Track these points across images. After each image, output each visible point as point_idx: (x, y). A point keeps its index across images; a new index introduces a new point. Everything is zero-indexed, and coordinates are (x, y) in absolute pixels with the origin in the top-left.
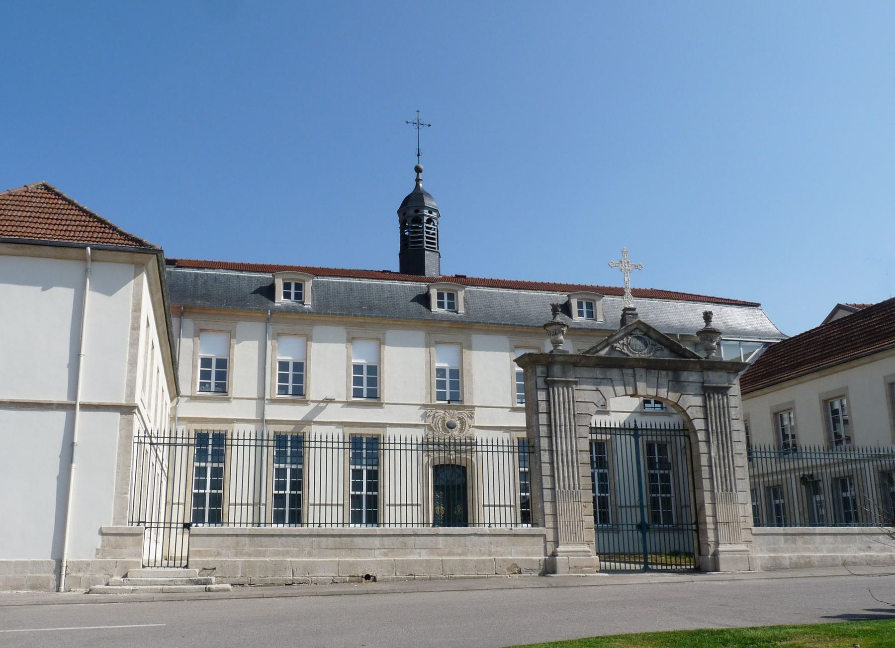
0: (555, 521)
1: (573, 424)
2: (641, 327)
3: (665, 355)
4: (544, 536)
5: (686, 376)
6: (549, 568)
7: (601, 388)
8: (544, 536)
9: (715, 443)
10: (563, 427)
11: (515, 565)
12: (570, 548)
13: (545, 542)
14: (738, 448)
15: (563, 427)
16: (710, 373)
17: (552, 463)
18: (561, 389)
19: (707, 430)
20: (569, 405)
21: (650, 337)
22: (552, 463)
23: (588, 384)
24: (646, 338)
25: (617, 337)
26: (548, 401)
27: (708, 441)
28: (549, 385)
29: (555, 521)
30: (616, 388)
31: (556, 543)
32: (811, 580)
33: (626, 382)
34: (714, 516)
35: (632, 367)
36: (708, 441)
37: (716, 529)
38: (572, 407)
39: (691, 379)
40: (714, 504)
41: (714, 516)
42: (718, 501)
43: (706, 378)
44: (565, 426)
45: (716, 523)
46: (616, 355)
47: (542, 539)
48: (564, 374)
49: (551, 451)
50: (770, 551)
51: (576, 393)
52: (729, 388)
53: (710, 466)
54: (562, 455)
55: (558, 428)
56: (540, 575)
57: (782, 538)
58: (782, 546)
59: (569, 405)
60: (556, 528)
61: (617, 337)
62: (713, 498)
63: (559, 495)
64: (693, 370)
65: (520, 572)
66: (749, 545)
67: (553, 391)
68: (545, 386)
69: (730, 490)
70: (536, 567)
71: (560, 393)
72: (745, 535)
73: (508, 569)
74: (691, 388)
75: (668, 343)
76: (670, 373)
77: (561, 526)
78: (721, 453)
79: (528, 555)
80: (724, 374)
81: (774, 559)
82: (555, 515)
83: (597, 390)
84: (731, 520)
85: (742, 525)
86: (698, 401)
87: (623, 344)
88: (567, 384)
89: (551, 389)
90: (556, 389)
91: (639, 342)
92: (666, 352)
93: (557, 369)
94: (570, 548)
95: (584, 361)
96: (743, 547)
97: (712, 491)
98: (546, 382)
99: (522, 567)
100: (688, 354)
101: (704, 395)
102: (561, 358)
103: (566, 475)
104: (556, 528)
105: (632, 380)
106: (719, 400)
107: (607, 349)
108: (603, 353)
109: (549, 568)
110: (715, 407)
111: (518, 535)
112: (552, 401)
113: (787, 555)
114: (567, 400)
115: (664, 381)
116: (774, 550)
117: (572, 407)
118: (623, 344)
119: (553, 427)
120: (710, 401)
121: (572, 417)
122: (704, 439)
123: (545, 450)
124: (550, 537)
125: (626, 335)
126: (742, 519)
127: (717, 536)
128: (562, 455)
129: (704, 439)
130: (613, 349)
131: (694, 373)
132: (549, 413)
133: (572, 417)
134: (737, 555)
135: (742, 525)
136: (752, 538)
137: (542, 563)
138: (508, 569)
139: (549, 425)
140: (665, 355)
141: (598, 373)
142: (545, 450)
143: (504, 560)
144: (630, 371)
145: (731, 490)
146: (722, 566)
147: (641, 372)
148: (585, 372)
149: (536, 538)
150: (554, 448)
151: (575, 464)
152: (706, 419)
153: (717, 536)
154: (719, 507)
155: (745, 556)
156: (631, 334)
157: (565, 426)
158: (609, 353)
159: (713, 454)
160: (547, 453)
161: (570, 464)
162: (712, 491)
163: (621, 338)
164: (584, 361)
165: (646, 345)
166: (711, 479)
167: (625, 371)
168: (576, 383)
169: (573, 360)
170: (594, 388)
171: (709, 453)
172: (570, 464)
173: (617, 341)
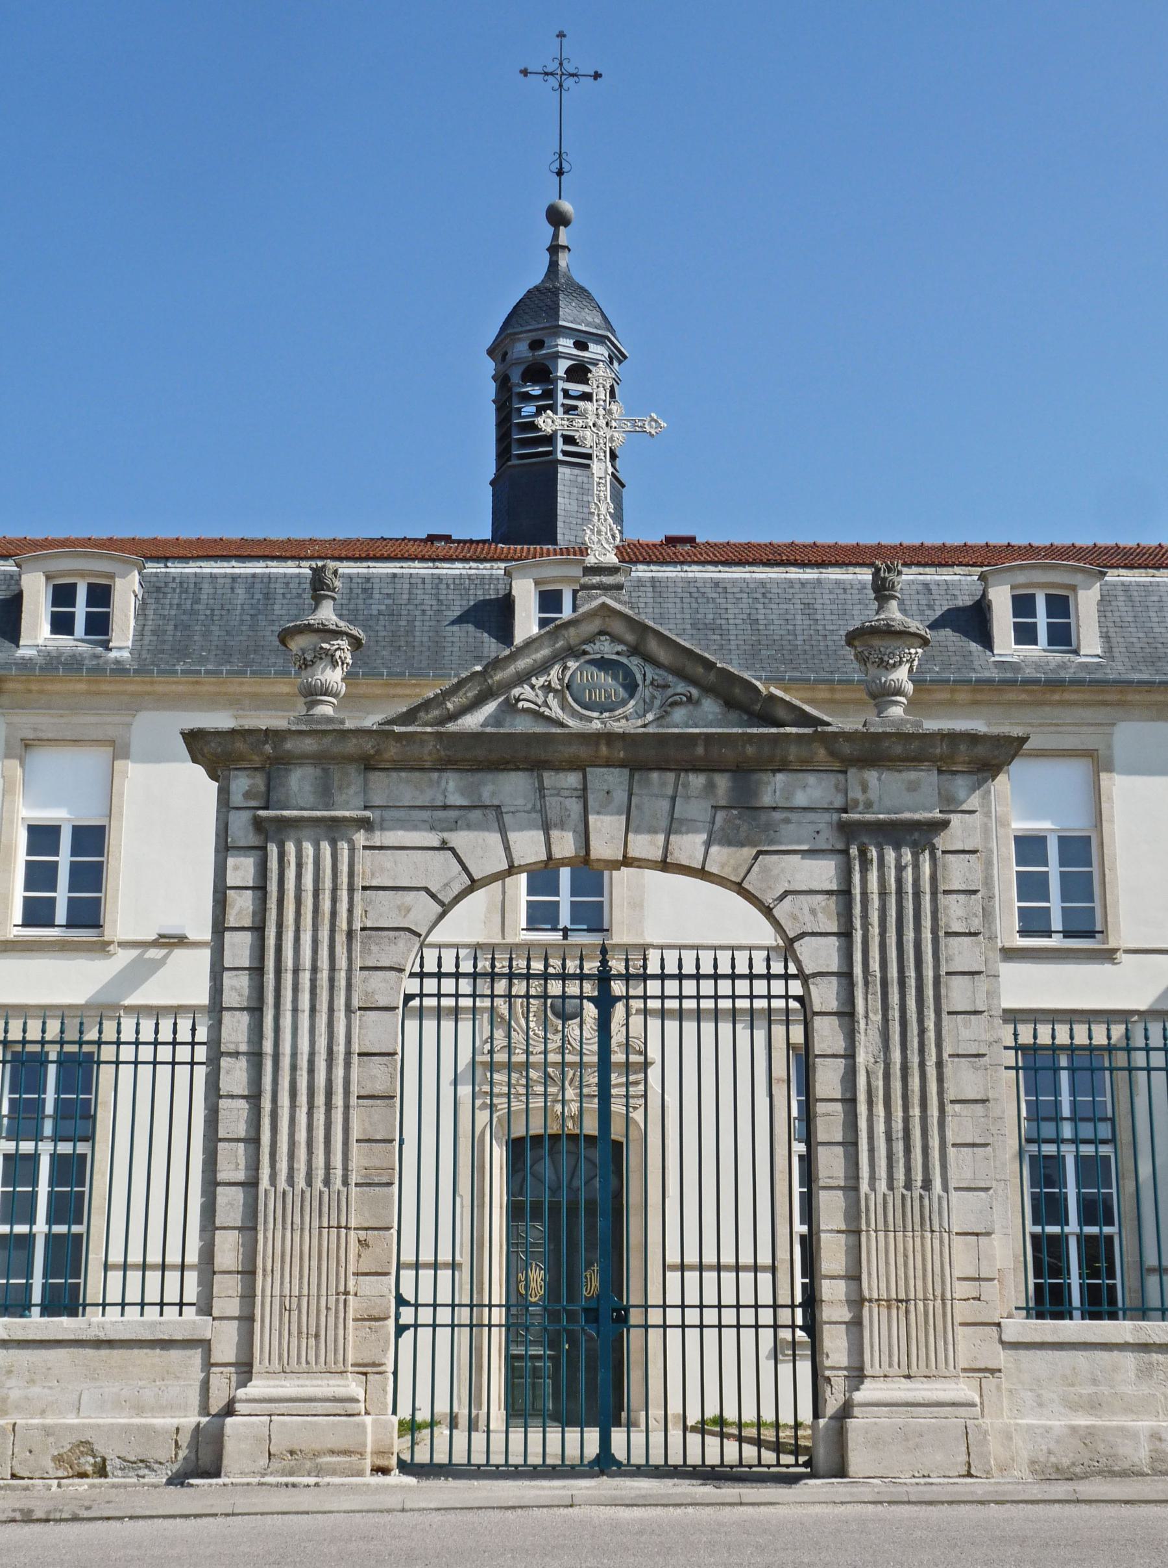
0: (248, 1297)
1: (342, 963)
2: (618, 627)
3: (705, 719)
4: (205, 1345)
5: (774, 788)
6: (203, 1459)
7: (459, 839)
8: (205, 1345)
9: (877, 1018)
10: (305, 977)
11: (86, 1447)
12: (289, 1387)
13: (208, 1365)
14: (965, 1033)
15: (305, 977)
16: (871, 776)
17: (254, 1098)
18: (308, 849)
19: (846, 975)
20: (334, 900)
21: (649, 659)
22: (254, 1098)
23: (404, 825)
24: (634, 663)
25: (522, 664)
26: (261, 889)
27: (847, 1015)
28: (270, 831)
29: (248, 1297)
30: (512, 836)
31: (245, 1369)
32: (1069, 1510)
33: (553, 815)
34: (854, 1277)
35: (577, 765)
36: (847, 1015)
37: (856, 1324)
38: (343, 907)
39: (800, 799)
40: (854, 1232)
41: (854, 1277)
42: (872, 1218)
43: (856, 793)
44: (315, 969)
45: (857, 1302)
46: (522, 726)
47: (196, 1356)
48: (326, 795)
49: (255, 1057)
50: (1074, 1406)
51: (365, 861)
52: (945, 824)
53: (850, 1102)
54: (294, 1068)
55: (288, 979)
56: (170, 1482)
57: (1129, 1360)
58: (1129, 1390)
59: (334, 900)
60: (247, 1319)
61: (522, 664)
62: (853, 1212)
63: (268, 1205)
64: (806, 766)
65: (102, 1472)
66: (990, 1382)
67: (282, 855)
68: (253, 840)
69: (919, 1186)
70: (164, 1452)
71: (304, 858)
72: (970, 1346)
73: (59, 1460)
74: (796, 833)
75: (712, 677)
76: (723, 782)
77: (266, 1310)
78: (896, 1056)
79: (140, 1410)
80: (927, 778)
81: (1087, 1436)
82: (248, 1273)
83: (444, 847)
84: (916, 1289)
85: (962, 1311)
86: (822, 873)
87: (547, 688)
88: (334, 829)
89: (273, 849)
90: (290, 847)
91: (604, 678)
92: (710, 706)
93: (299, 781)
94: (289, 1387)
95: (393, 751)
96: (964, 1390)
97: (851, 1188)
98: (259, 825)
99: (110, 1451)
100: (781, 713)
101: (846, 852)
102: (309, 745)
103: (302, 1136)
104: (247, 1319)
105: (575, 806)
106: (900, 869)
107: (490, 707)
108: (472, 721)
109: (203, 1459)
110: (883, 894)
111: (110, 1344)
112: (273, 887)
113: (1144, 1424)
114: (328, 884)
115: (696, 809)
116: (1094, 1405)
117: (343, 907)
118: (547, 688)
119: (270, 977)
120: (864, 870)
121: (341, 938)
122: (833, 1005)
123: (236, 1054)
124: (226, 1349)
125: (559, 657)
126: (963, 1289)
127: (857, 1348)
128: (294, 1068)
129: (833, 1005)
130: (510, 707)
131: (811, 779)
132: (259, 929)
133: (341, 938)
134: (924, 1420)
135: (962, 1311)
136: (1002, 1358)
137: (185, 1439)
138: (59, 1460)
139: (257, 971)
140: (705, 719)
141: (452, 788)
142: (236, 1054)
143: (47, 1431)
144: (572, 779)
145: (927, 1184)
146: (857, 1460)
147: (611, 780)
148: (403, 789)
149: (175, 1354)
150: (268, 1046)
151: (338, 1100)
152: (846, 935)
153: (857, 1348)
154: (871, 1243)
155: (954, 1421)
156: (573, 652)
157: (315, 969)
158: (496, 719)
159: (862, 1058)
160: (243, 1062)
161: (320, 1100)
162: (851, 1188)
163: (543, 668)
164: (393, 751)
165: (631, 688)
166: (850, 1144)
167: (549, 778)
168: (366, 824)
169: (351, 746)
170: (433, 839)
171: (850, 1055)
172: (320, 1100)
173: (523, 678)
